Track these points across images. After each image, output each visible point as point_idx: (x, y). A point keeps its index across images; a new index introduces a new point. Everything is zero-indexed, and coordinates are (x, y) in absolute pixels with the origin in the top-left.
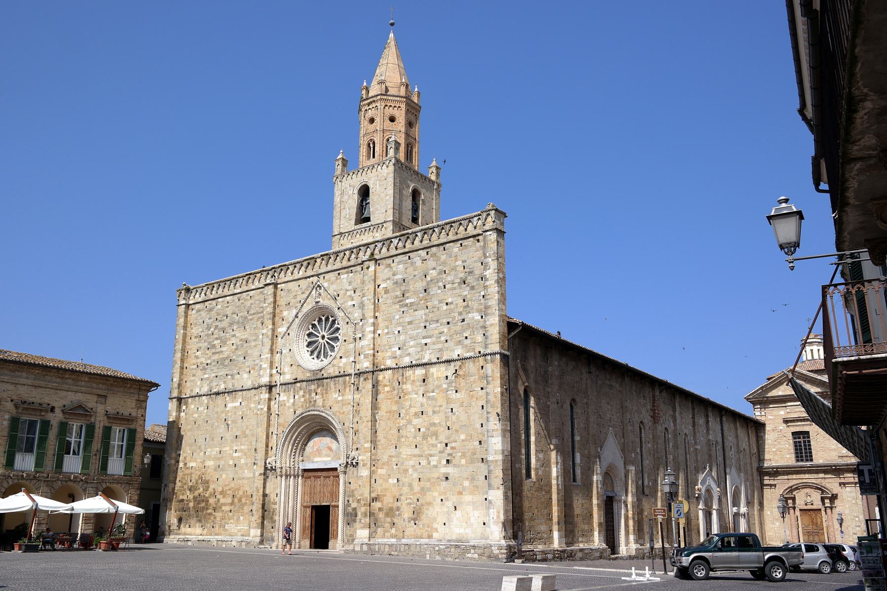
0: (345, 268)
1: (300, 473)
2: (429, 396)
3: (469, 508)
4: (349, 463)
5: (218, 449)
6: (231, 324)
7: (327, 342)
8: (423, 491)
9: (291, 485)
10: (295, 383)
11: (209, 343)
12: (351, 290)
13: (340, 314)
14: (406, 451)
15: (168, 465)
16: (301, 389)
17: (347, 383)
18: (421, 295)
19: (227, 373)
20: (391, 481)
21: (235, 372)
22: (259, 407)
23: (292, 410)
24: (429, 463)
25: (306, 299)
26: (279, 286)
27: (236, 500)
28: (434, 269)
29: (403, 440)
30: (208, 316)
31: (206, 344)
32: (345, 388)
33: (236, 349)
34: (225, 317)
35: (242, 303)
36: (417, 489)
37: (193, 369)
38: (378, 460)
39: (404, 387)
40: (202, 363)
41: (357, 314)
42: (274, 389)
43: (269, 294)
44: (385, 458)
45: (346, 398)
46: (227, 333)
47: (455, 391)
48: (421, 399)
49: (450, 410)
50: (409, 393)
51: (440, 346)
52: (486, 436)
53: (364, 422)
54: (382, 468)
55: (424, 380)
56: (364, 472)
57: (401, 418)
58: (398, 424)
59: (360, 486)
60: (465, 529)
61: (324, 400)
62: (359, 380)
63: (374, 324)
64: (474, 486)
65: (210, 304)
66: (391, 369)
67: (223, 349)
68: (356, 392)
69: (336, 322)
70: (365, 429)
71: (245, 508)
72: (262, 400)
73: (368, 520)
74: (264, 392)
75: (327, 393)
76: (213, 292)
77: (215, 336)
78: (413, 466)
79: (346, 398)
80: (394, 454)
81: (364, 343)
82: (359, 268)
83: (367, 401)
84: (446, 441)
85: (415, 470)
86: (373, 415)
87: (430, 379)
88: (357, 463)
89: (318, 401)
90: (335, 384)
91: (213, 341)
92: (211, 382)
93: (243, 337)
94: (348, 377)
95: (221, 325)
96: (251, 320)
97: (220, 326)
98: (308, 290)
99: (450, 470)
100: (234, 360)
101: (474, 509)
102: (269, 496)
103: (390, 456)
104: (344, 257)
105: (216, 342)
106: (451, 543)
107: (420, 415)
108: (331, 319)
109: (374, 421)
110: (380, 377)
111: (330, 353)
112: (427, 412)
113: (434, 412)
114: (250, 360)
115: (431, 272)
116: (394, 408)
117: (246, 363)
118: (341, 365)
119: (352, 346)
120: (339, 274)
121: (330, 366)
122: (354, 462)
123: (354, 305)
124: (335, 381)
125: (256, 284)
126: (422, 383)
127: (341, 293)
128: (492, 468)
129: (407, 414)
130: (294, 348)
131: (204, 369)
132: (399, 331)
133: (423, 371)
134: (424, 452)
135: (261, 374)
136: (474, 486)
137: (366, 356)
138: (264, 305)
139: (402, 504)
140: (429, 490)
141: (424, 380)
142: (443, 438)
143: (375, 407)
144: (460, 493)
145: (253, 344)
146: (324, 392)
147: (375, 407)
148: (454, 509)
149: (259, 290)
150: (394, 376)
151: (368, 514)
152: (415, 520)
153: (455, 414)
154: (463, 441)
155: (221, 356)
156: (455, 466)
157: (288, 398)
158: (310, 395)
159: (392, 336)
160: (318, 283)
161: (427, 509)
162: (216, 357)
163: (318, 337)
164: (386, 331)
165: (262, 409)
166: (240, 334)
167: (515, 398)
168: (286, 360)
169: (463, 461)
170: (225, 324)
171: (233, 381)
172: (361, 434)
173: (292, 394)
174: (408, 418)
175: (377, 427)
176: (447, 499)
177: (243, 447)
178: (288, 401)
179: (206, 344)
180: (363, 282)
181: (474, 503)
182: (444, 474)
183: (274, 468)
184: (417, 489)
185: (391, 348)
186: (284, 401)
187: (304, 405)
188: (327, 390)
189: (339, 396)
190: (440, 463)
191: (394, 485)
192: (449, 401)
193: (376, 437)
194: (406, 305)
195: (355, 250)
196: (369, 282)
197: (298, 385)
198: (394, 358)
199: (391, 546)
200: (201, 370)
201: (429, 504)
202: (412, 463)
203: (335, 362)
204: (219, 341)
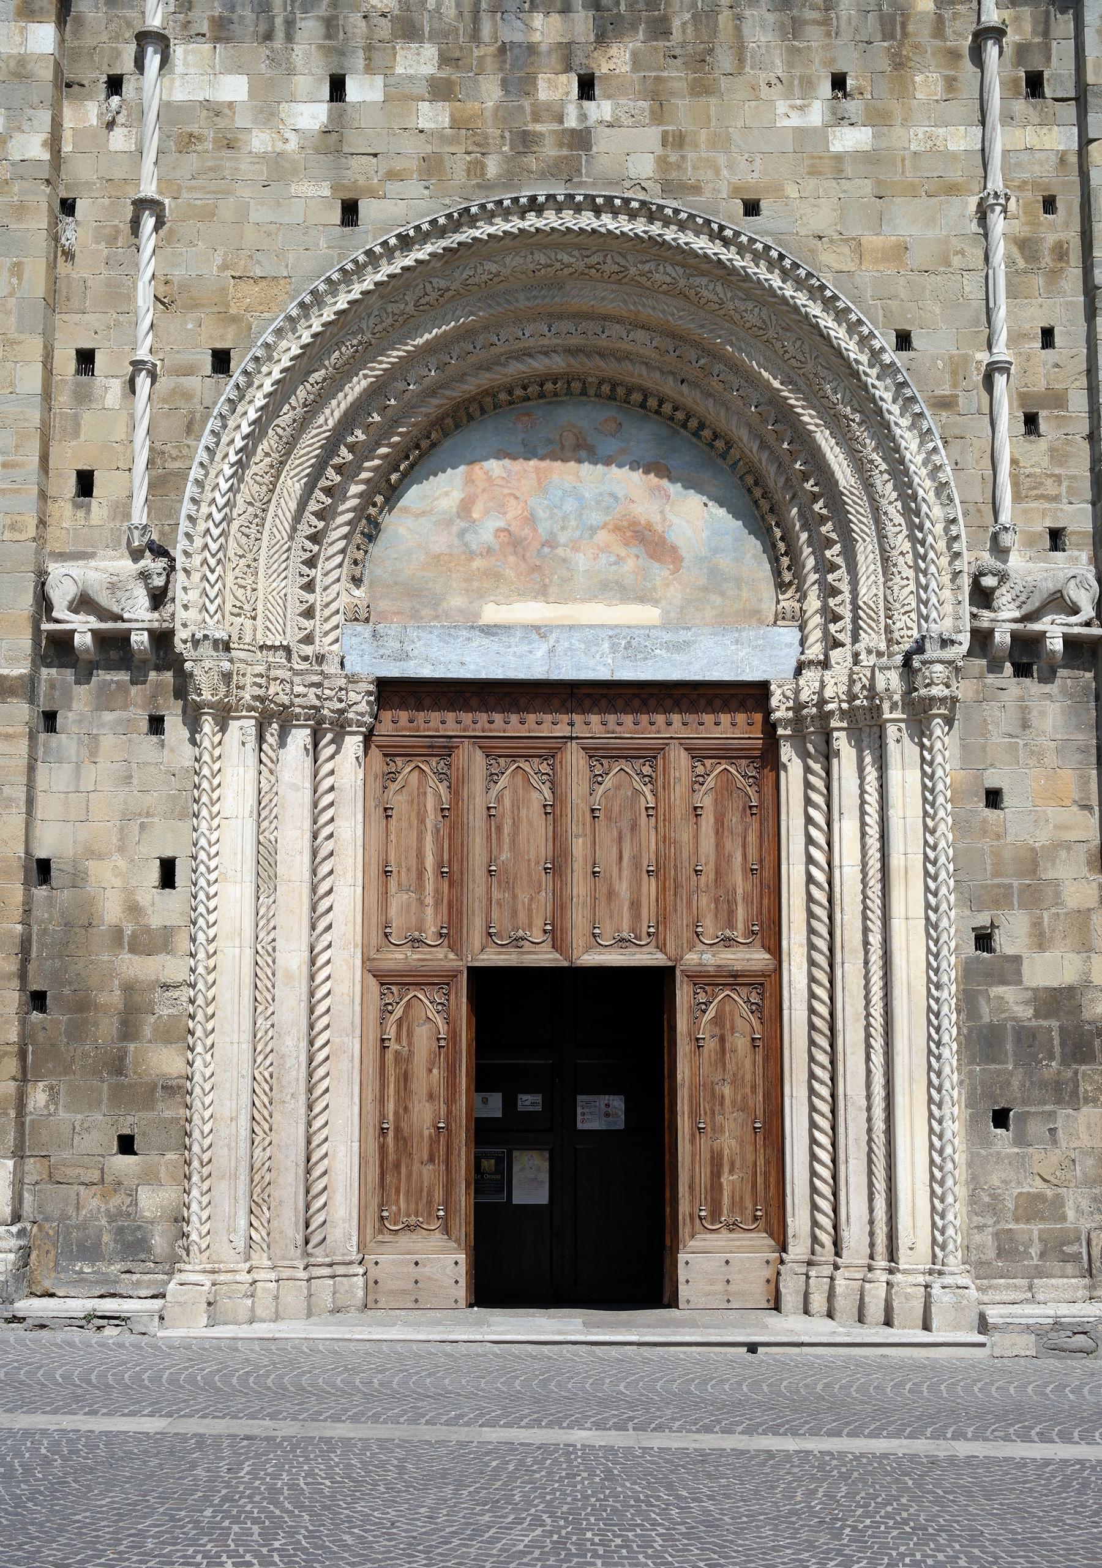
4: (1002, 637)
17: (921, 32)
32: (899, 63)
61: (675, 141)
68: (1021, 106)
89: (604, 143)
102: (78, 879)
146: (676, 76)
187: (458, 167)
189: (841, 120)
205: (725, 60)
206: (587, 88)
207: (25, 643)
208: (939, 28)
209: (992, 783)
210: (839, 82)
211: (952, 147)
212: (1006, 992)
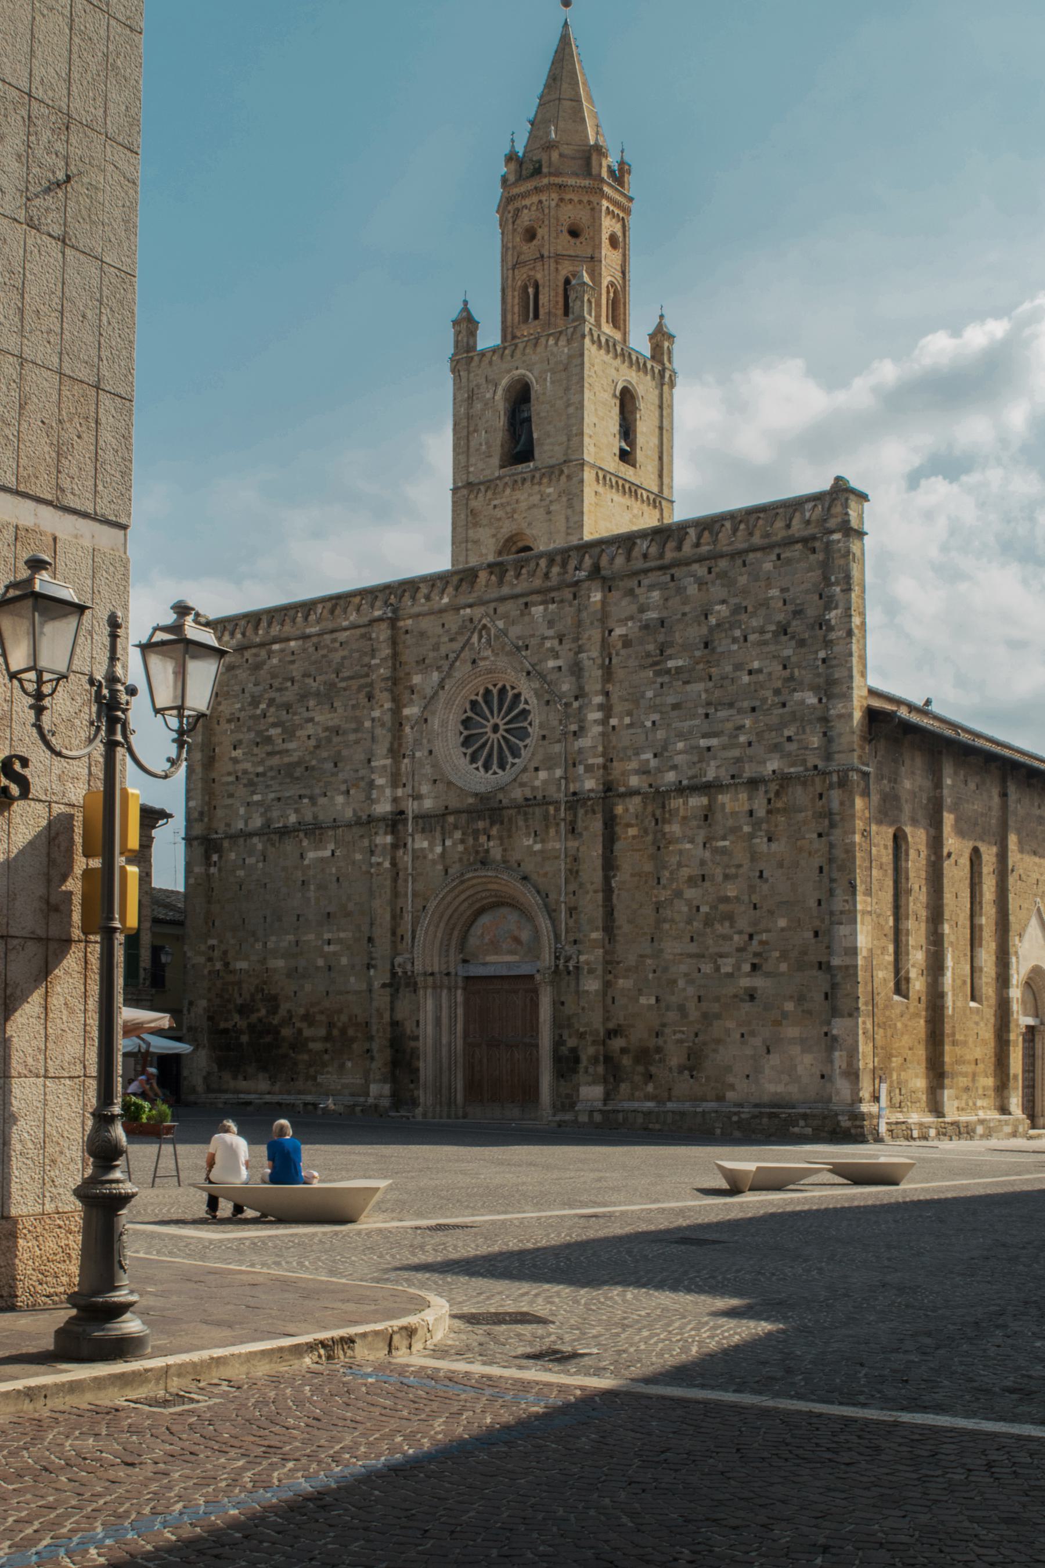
0: (538, 592)
1: (460, 984)
2: (717, 848)
3: (795, 1050)
4: (561, 967)
5: (291, 938)
6: (303, 697)
7: (504, 737)
8: (707, 1018)
9: (444, 1005)
10: (444, 815)
11: (259, 733)
12: (552, 638)
13: (526, 689)
14: (671, 948)
15: (193, 966)
16: (456, 827)
18: (698, 653)
19: (302, 792)
20: (643, 1000)
21: (317, 791)
22: (374, 859)
23: (440, 867)
24: (717, 969)
25: (461, 652)
26: (401, 624)
27: (335, 1032)
28: (723, 602)
29: (666, 926)
30: (253, 678)
31: (252, 735)
32: (547, 827)
33: (317, 747)
34: (289, 684)
35: (324, 656)
36: (694, 1014)
37: (228, 783)
38: (618, 963)
39: (667, 828)
40: (245, 772)
41: (566, 686)
42: (400, 827)
43: (381, 638)
44: (632, 960)
45: (550, 845)
46: (295, 714)
47: (765, 839)
48: (699, 852)
49: (758, 874)
50: (677, 841)
51: (736, 753)
52: (827, 922)
53: (587, 893)
54: (626, 977)
55: (706, 817)
56: (592, 985)
57: (661, 886)
58: (656, 897)
59: (583, 1009)
60: (786, 1085)
61: (505, 850)
62: (575, 815)
63: (601, 707)
64: (803, 1011)
65: (256, 655)
66: (639, 793)
67: (291, 746)
68: (570, 836)
69: (522, 699)
70: (591, 904)
71: (355, 1046)
72: (380, 848)
73: (601, 1069)
74: (381, 831)
75: (510, 836)
76: (261, 632)
77: (271, 720)
78: (686, 975)
79: (550, 845)
80: (648, 951)
81: (585, 742)
82: (567, 594)
83: (594, 853)
84: (750, 930)
85: (690, 982)
86: (607, 880)
87: (719, 816)
88: (577, 968)
89: (492, 852)
90: (526, 820)
91: (267, 730)
92: (268, 809)
93: (330, 724)
94: (551, 809)
95: (280, 698)
96: (345, 689)
97: (279, 700)
98: (462, 634)
99: (758, 982)
100: (313, 768)
101: (803, 1051)
103: (641, 956)
104: (535, 571)
105: (273, 732)
106: (763, 1110)
107: (699, 883)
108: (510, 694)
109: (608, 891)
110: (619, 810)
111: (510, 760)
112: (713, 875)
113: (726, 877)
114: (348, 767)
115: (718, 608)
116: (648, 867)
117: (340, 775)
118: (537, 783)
119: (557, 748)
120: (526, 604)
121: (517, 784)
122: (571, 965)
123: (560, 668)
124: (526, 814)
125: (352, 618)
126: (702, 823)
127: (533, 642)
128: (839, 979)
129: (671, 880)
130: (439, 747)
131: (251, 784)
132: (654, 723)
133: (705, 801)
134: (707, 949)
135: (374, 796)
136: (803, 1011)
137: (589, 769)
138: (373, 662)
139: (665, 1042)
140: (718, 1016)
141: (706, 817)
142: (742, 923)
143: (609, 864)
144: (777, 1023)
145: (352, 737)
146: (505, 834)
147: (609, 864)
148: (765, 1051)
149: (358, 632)
150: (645, 808)
151: (601, 1058)
152: (691, 1069)
153: (767, 881)
154: (783, 930)
155: (286, 760)
156: (768, 975)
157: (432, 845)
158: (476, 839)
159: (639, 730)
160: (484, 621)
161: (715, 1051)
162: (275, 761)
163: (486, 726)
164: (627, 720)
165: (379, 864)
166: (323, 717)
167: (879, 851)
168: (424, 771)
169: (783, 967)
170: (290, 695)
171: (315, 809)
172: (582, 915)
173: (438, 835)
174: (674, 886)
175: (615, 901)
176: (753, 1033)
177: (342, 935)
178: (432, 850)
179: (252, 735)
180: (579, 624)
181: (802, 1041)
182: (746, 989)
183: (409, 973)
184: (694, 1014)
185: (637, 754)
186: (422, 849)
188: (509, 830)
189: (535, 842)
190: (739, 969)
191: (650, 1007)
192: (754, 857)
193: (613, 921)
194: (668, 671)
195: (558, 559)
196: (592, 623)
197: (451, 819)
198: (644, 773)
199: (648, 1114)
200: (245, 786)
201: (718, 1041)
202: (683, 968)
203: (525, 778)
204: (279, 730)
205: (514, 829)
206: (489, 840)
207: (388, 975)
208: (555, 819)
209: (562, 999)
210: (536, 835)
211: (558, 847)
212: (563, 1048)
